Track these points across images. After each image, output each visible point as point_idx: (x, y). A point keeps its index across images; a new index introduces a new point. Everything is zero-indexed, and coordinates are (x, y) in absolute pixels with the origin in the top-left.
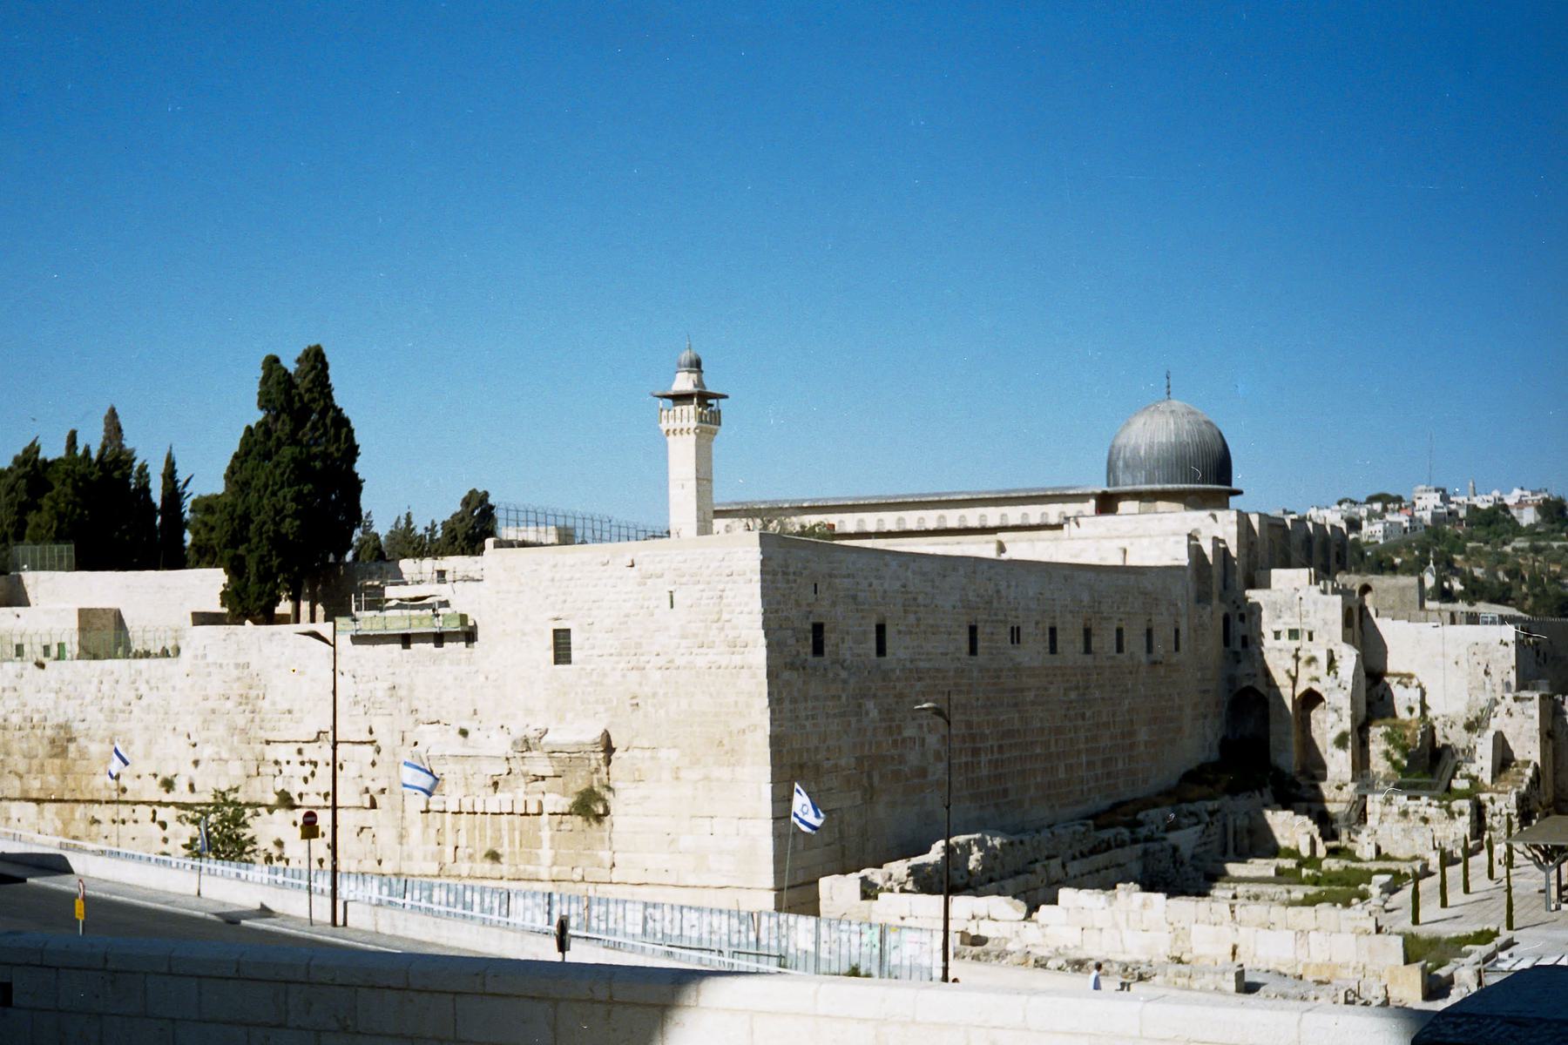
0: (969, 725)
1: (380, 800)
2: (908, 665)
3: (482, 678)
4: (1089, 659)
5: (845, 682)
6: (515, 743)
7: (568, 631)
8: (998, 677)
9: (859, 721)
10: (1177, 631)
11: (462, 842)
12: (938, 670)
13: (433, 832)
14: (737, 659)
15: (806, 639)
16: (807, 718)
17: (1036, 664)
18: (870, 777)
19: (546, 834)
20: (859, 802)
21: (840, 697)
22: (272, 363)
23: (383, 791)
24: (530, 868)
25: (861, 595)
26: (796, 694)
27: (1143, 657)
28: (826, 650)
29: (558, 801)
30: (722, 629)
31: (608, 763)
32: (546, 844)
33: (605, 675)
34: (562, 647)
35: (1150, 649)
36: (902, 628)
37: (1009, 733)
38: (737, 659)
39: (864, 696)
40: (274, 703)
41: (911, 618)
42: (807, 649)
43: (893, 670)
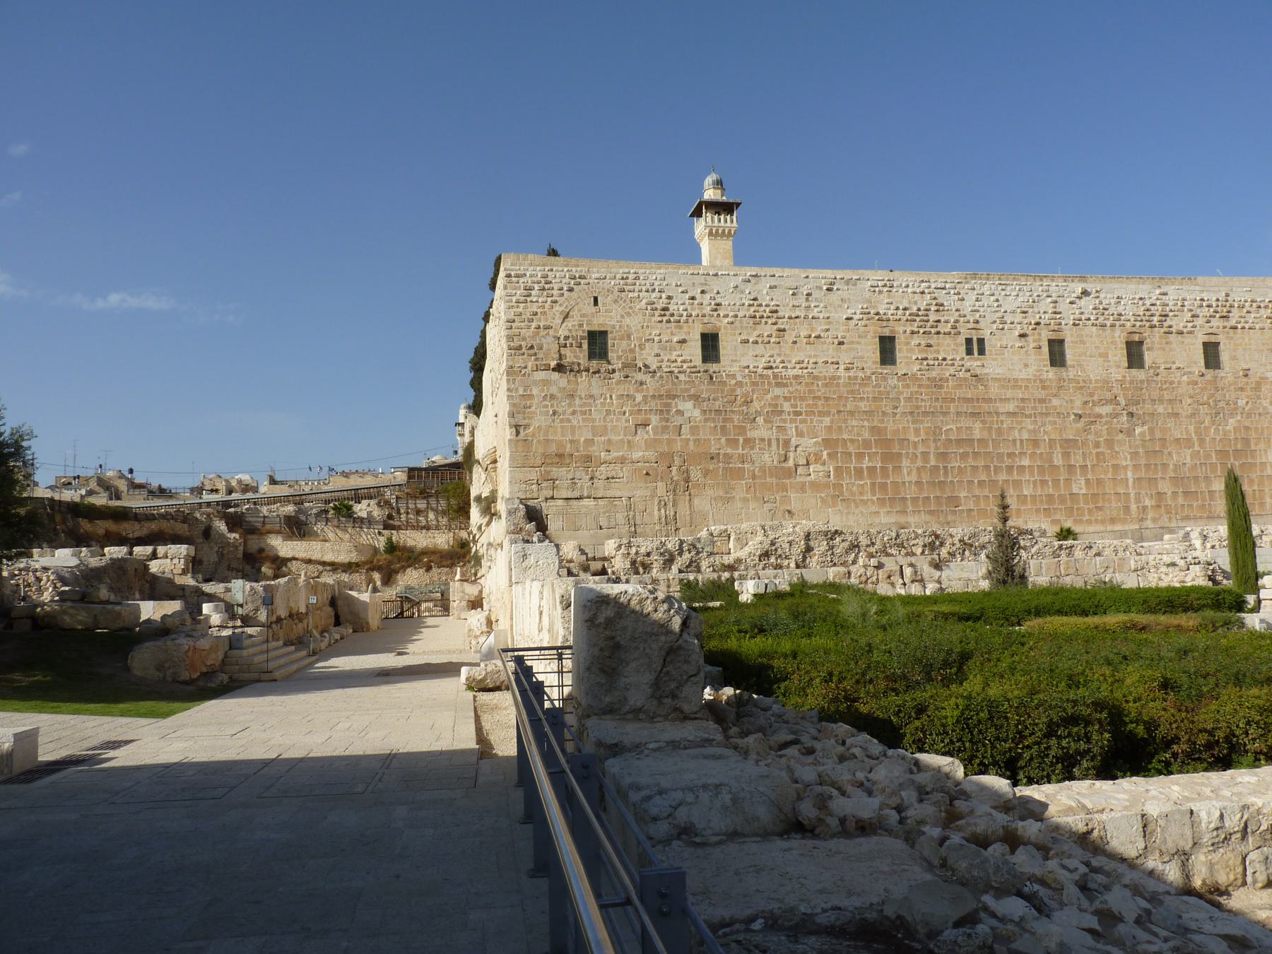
2: (760, 370)
5: (641, 384)
8: (941, 387)
12: (816, 378)
15: (580, 346)
16: (574, 413)
17: (1023, 376)
25: (672, 307)
26: (554, 390)
39: (674, 397)
41: (767, 329)
42: (578, 355)
43: (734, 376)
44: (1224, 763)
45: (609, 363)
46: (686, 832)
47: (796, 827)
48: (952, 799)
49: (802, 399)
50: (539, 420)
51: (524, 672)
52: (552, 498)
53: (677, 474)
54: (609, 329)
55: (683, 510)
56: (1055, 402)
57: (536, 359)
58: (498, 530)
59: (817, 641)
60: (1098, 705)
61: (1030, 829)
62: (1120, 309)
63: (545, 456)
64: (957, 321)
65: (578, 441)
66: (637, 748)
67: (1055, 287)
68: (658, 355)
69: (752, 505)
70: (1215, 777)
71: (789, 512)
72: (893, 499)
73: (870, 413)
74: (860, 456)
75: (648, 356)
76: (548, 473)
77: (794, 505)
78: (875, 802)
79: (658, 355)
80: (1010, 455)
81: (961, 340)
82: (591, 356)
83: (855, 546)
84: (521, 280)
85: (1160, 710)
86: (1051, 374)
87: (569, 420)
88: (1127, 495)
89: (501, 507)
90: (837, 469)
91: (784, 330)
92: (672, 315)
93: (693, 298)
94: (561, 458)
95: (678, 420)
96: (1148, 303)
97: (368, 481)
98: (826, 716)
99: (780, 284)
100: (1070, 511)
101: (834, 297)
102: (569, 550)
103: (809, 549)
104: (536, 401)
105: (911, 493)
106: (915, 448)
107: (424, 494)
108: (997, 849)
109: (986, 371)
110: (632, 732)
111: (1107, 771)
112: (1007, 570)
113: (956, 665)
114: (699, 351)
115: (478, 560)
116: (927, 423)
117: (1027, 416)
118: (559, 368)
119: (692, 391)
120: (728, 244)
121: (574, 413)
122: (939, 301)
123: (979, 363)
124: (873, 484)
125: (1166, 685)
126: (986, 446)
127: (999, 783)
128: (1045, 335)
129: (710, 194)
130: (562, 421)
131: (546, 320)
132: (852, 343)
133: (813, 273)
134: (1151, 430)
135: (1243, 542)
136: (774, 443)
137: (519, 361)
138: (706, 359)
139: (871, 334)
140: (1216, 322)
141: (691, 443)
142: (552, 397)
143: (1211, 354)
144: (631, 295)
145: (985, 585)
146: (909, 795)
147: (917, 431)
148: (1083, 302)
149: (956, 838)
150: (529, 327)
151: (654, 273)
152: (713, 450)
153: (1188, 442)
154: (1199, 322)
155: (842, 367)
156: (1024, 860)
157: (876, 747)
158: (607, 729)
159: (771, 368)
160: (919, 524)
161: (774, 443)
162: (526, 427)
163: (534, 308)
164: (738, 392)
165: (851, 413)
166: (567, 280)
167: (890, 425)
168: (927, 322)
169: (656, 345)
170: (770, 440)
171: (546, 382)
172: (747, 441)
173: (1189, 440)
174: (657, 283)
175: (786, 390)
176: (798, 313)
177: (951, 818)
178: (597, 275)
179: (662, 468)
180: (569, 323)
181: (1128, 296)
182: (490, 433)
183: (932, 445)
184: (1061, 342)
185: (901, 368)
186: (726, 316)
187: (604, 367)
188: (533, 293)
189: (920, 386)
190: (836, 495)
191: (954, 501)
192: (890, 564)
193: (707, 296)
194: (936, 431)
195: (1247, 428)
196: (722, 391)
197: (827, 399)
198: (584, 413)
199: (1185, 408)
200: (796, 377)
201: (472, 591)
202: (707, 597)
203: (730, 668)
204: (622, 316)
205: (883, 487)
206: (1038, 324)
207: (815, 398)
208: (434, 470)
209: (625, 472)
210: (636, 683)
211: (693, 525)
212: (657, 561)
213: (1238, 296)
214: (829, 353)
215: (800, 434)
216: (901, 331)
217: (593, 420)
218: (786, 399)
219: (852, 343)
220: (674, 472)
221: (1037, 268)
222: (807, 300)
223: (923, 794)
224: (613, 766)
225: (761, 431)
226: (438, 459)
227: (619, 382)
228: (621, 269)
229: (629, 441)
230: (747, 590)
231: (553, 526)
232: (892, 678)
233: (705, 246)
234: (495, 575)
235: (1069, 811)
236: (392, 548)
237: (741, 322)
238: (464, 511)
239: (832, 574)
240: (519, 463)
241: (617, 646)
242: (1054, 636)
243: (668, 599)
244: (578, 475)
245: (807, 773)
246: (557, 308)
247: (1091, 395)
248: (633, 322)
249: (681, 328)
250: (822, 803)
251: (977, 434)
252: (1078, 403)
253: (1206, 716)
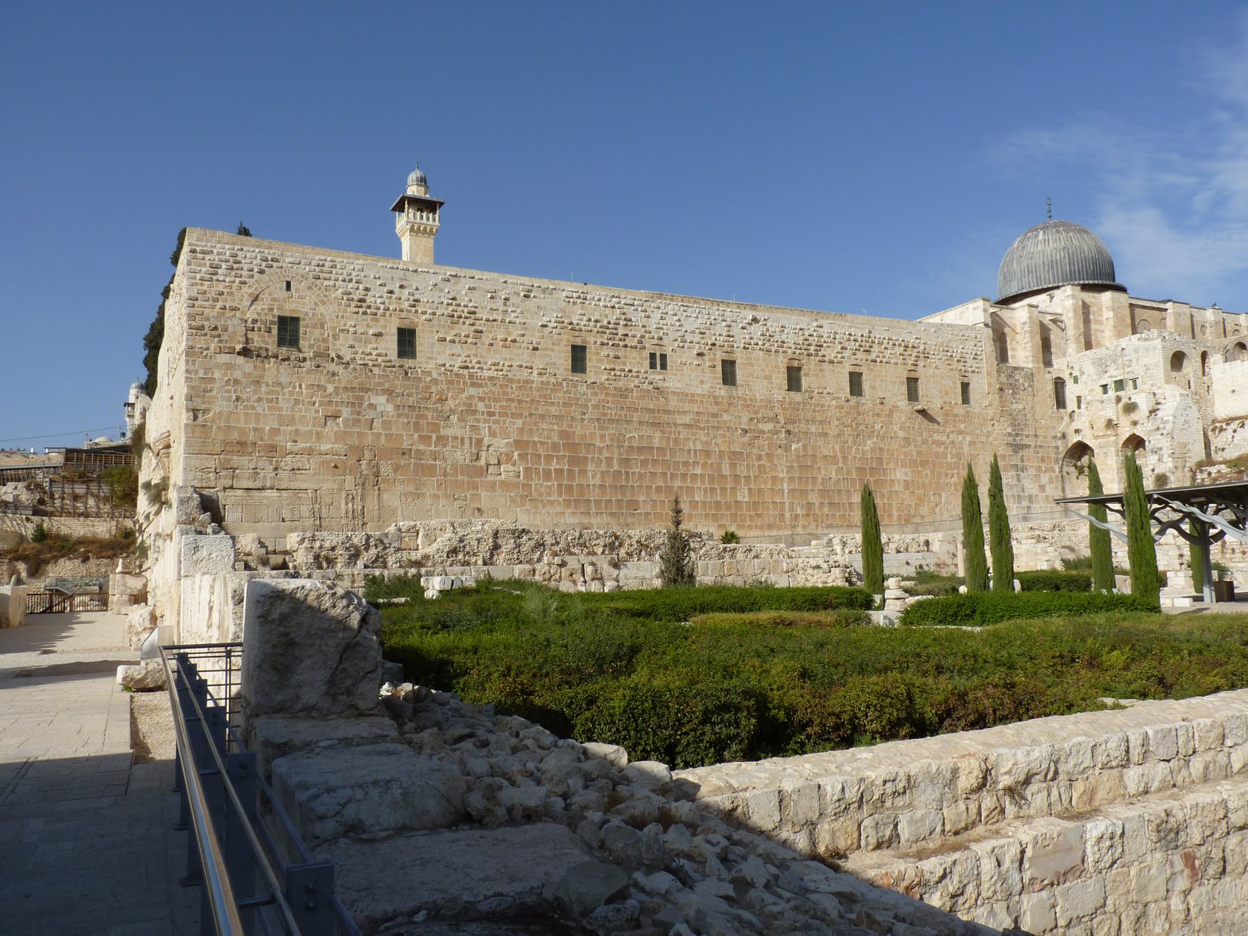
0: (562, 434)
2: (456, 369)
4: (796, 397)
5: (333, 374)
8: (626, 397)
10: (965, 386)
12: (511, 381)
15: (269, 331)
16: (259, 400)
17: (699, 391)
25: (369, 299)
26: (238, 374)
27: (903, 403)
28: (303, 343)
35: (913, 395)
37: (640, 449)
39: (368, 390)
41: (465, 330)
42: (267, 341)
43: (429, 373)
44: (847, 742)
45: (300, 351)
46: (354, 830)
47: (465, 819)
48: (614, 783)
49: (496, 400)
50: (220, 405)
51: (187, 669)
52: (231, 487)
53: (367, 468)
54: (301, 316)
55: (372, 505)
56: (726, 417)
57: (220, 342)
58: (168, 519)
59: (498, 636)
60: (747, 694)
61: (682, 808)
62: (784, 337)
63: (225, 443)
64: (643, 337)
65: (263, 429)
66: (308, 746)
67: (730, 312)
68: (352, 347)
69: (442, 502)
70: (840, 755)
71: (479, 510)
72: (578, 500)
73: (559, 418)
74: (549, 458)
75: (341, 347)
76: (228, 461)
77: (484, 503)
78: (542, 791)
79: (352, 347)
80: (686, 464)
81: (646, 354)
82: (281, 342)
83: (540, 545)
84: (208, 257)
85: (798, 697)
86: (723, 391)
87: (253, 408)
88: (783, 503)
89: (173, 495)
90: (527, 470)
91: (481, 332)
92: (369, 307)
93: (391, 292)
94: (242, 446)
95: (371, 414)
96: (807, 333)
97: (17, 462)
98: (502, 710)
99: (480, 287)
100: (734, 517)
101: (531, 304)
102: (247, 542)
103: (496, 547)
104: (217, 385)
105: (594, 495)
106: (601, 453)
107: (84, 478)
108: (652, 829)
109: (667, 385)
110: (303, 730)
111: (751, 754)
112: (678, 571)
113: (627, 658)
114: (395, 346)
115: (144, 551)
116: (612, 430)
117: (701, 429)
118: (245, 352)
119: (386, 386)
120: (429, 242)
121: (259, 400)
122: (628, 316)
123: (661, 377)
124: (560, 486)
125: (805, 674)
126: (665, 455)
127: (656, 767)
128: (720, 355)
129: (413, 190)
130: (246, 407)
131: (233, 301)
132: (546, 349)
133: (511, 279)
134: (805, 447)
135: (873, 549)
136: (467, 442)
137: (200, 342)
138: (401, 354)
139: (565, 342)
140: (860, 355)
141: (383, 438)
142: (236, 382)
143: (855, 382)
144: (326, 283)
145: (658, 583)
146: (575, 783)
147: (602, 437)
148: (753, 328)
149: (616, 821)
150: (213, 307)
151: (351, 263)
152: (405, 446)
153: (834, 460)
154: (847, 353)
155: (535, 372)
156: (675, 838)
157: (547, 737)
158: (276, 728)
159: (467, 367)
160: (601, 525)
161: (467, 442)
162: (206, 411)
163: (221, 287)
164: (433, 389)
165: (542, 417)
166: (258, 261)
167: (578, 430)
168: (616, 334)
169: (350, 336)
170: (462, 439)
171: (229, 366)
172: (440, 438)
173: (835, 457)
174: (354, 274)
175: (481, 390)
176: (495, 317)
177: (613, 802)
178: (290, 260)
179: (351, 461)
180: (258, 307)
181: (791, 325)
182: (165, 416)
183: (616, 451)
184: (733, 363)
185: (590, 376)
186: (424, 313)
187: (294, 354)
188: (220, 271)
189: (607, 394)
190: (526, 496)
191: (634, 504)
192: (573, 563)
193: (406, 291)
194: (620, 439)
195: (881, 449)
196: (417, 388)
197: (520, 401)
198: (271, 401)
199: (833, 430)
200: (491, 378)
201: (135, 584)
202: (390, 595)
203: (411, 664)
204: (316, 304)
205: (569, 488)
206: (713, 345)
207: (508, 400)
208: (96, 452)
209: (312, 464)
210: (310, 680)
211: (381, 520)
212: (341, 556)
213: (878, 334)
214: (523, 357)
215: (493, 434)
216: (592, 342)
217: (280, 409)
218: (481, 399)
219: (546, 349)
220: (363, 467)
221: (715, 293)
222: (505, 304)
223: (588, 780)
224: (281, 766)
225: (454, 429)
226: (102, 441)
227: (309, 372)
228: (317, 255)
229: (318, 433)
230: (433, 587)
231: (230, 517)
232: (567, 672)
233: (406, 242)
234: (162, 569)
235: (718, 790)
236: (41, 535)
237: (439, 320)
238: (130, 498)
239: (518, 571)
240: (193, 449)
241: (291, 644)
242: (714, 631)
243: (348, 595)
244: (261, 465)
245: (479, 765)
246: (245, 289)
247: (756, 413)
248: (328, 311)
249: (377, 321)
250: (491, 793)
251: (656, 443)
252: (745, 419)
253: (834, 702)
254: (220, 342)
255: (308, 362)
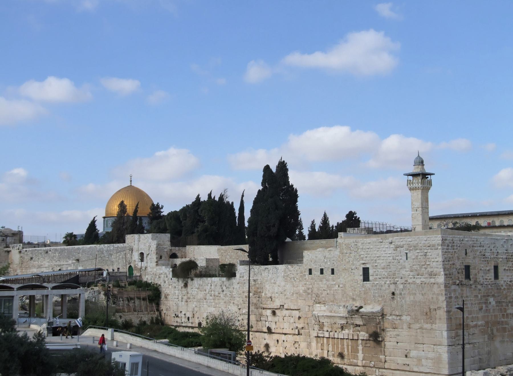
1: (302, 331)
2: (509, 282)
3: (337, 286)
5: (480, 290)
6: (349, 312)
7: (368, 268)
9: (487, 307)
11: (330, 349)
13: (320, 345)
14: (432, 280)
18: (492, 330)
19: (360, 348)
20: (486, 340)
21: (477, 296)
22: (267, 169)
23: (303, 328)
24: (355, 361)
25: (486, 254)
26: (457, 295)
28: (471, 277)
29: (363, 335)
30: (426, 268)
31: (383, 320)
32: (361, 352)
33: (382, 286)
34: (366, 275)
36: (507, 268)
38: (432, 280)
39: (488, 296)
40: (265, 294)
42: (462, 277)
45: (470, 280)
57: (452, 280)
63: (456, 325)
114: (493, 274)
119: (493, 293)
144: (476, 248)
164: (504, 292)
171: (455, 290)
174: (482, 243)
178: (466, 239)
188: (450, 247)
209: (476, 331)
227: (475, 290)
246: (456, 255)
249: (488, 263)
254: (452, 280)
255: (473, 286)
